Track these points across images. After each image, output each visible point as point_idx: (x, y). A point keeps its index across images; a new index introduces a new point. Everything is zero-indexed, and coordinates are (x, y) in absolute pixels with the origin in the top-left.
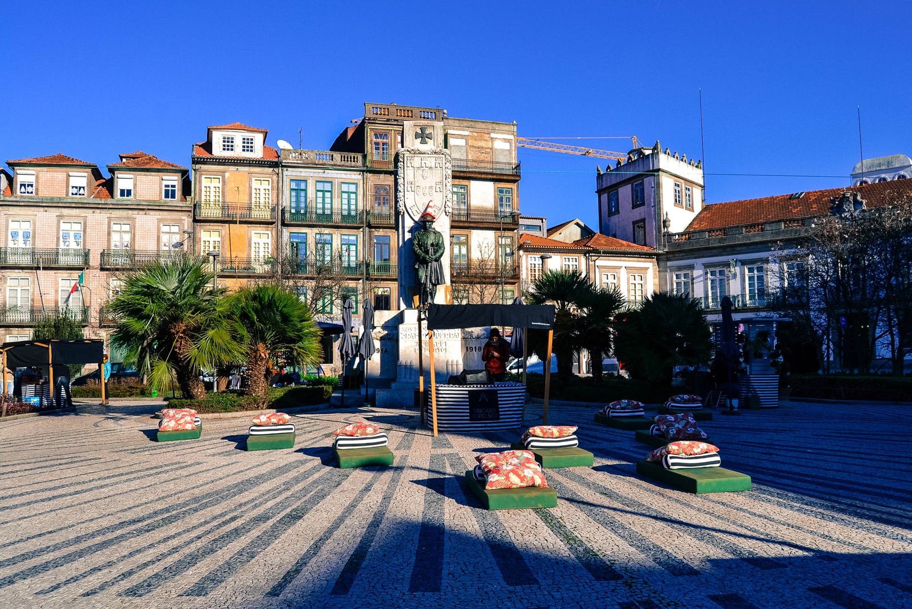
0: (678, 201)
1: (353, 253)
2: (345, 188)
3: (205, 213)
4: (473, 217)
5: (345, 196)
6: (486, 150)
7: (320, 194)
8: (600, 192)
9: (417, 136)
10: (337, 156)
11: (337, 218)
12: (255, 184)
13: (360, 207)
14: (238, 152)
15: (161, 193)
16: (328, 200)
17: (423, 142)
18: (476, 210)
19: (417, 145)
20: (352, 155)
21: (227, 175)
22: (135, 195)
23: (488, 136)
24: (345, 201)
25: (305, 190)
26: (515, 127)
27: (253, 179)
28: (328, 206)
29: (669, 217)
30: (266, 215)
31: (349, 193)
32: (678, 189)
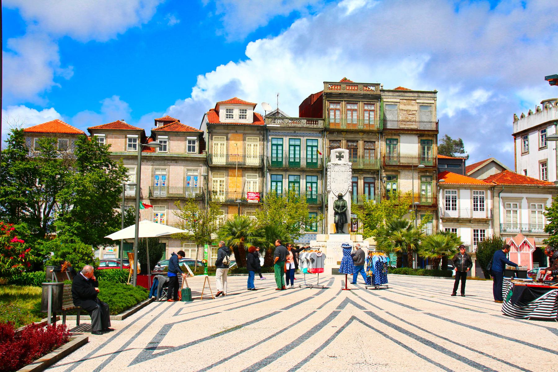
2: (310, 143)
5: (309, 149)
6: (413, 112)
7: (292, 148)
9: (337, 157)
11: (303, 164)
14: (236, 119)
15: (185, 148)
16: (297, 152)
17: (340, 159)
18: (403, 157)
19: (337, 161)
21: (230, 135)
22: (169, 150)
23: (414, 101)
24: (309, 153)
25: (282, 145)
27: (247, 138)
28: (297, 156)
31: (312, 147)
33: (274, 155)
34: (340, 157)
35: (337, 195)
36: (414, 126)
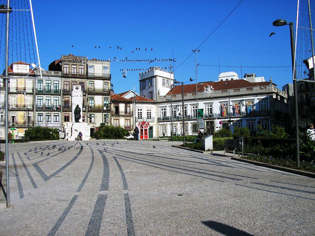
0: (163, 84)
1: (58, 103)
2: (55, 82)
3: (11, 91)
4: (96, 92)
8: (140, 81)
10: (53, 72)
12: (27, 81)
13: (60, 88)
17: (77, 90)
20: (57, 72)
26: (110, 62)
29: (160, 91)
30: (31, 91)
32: (164, 81)
33: (39, 88)
34: (77, 88)
35: (76, 105)
36: (101, 75)
